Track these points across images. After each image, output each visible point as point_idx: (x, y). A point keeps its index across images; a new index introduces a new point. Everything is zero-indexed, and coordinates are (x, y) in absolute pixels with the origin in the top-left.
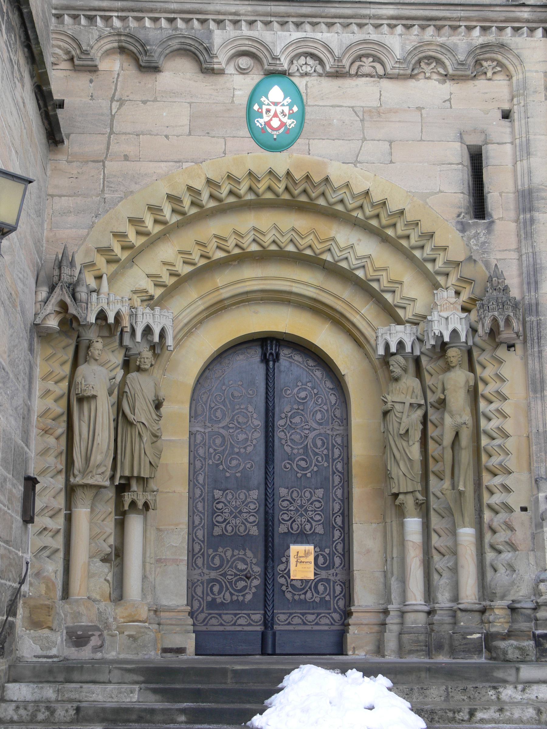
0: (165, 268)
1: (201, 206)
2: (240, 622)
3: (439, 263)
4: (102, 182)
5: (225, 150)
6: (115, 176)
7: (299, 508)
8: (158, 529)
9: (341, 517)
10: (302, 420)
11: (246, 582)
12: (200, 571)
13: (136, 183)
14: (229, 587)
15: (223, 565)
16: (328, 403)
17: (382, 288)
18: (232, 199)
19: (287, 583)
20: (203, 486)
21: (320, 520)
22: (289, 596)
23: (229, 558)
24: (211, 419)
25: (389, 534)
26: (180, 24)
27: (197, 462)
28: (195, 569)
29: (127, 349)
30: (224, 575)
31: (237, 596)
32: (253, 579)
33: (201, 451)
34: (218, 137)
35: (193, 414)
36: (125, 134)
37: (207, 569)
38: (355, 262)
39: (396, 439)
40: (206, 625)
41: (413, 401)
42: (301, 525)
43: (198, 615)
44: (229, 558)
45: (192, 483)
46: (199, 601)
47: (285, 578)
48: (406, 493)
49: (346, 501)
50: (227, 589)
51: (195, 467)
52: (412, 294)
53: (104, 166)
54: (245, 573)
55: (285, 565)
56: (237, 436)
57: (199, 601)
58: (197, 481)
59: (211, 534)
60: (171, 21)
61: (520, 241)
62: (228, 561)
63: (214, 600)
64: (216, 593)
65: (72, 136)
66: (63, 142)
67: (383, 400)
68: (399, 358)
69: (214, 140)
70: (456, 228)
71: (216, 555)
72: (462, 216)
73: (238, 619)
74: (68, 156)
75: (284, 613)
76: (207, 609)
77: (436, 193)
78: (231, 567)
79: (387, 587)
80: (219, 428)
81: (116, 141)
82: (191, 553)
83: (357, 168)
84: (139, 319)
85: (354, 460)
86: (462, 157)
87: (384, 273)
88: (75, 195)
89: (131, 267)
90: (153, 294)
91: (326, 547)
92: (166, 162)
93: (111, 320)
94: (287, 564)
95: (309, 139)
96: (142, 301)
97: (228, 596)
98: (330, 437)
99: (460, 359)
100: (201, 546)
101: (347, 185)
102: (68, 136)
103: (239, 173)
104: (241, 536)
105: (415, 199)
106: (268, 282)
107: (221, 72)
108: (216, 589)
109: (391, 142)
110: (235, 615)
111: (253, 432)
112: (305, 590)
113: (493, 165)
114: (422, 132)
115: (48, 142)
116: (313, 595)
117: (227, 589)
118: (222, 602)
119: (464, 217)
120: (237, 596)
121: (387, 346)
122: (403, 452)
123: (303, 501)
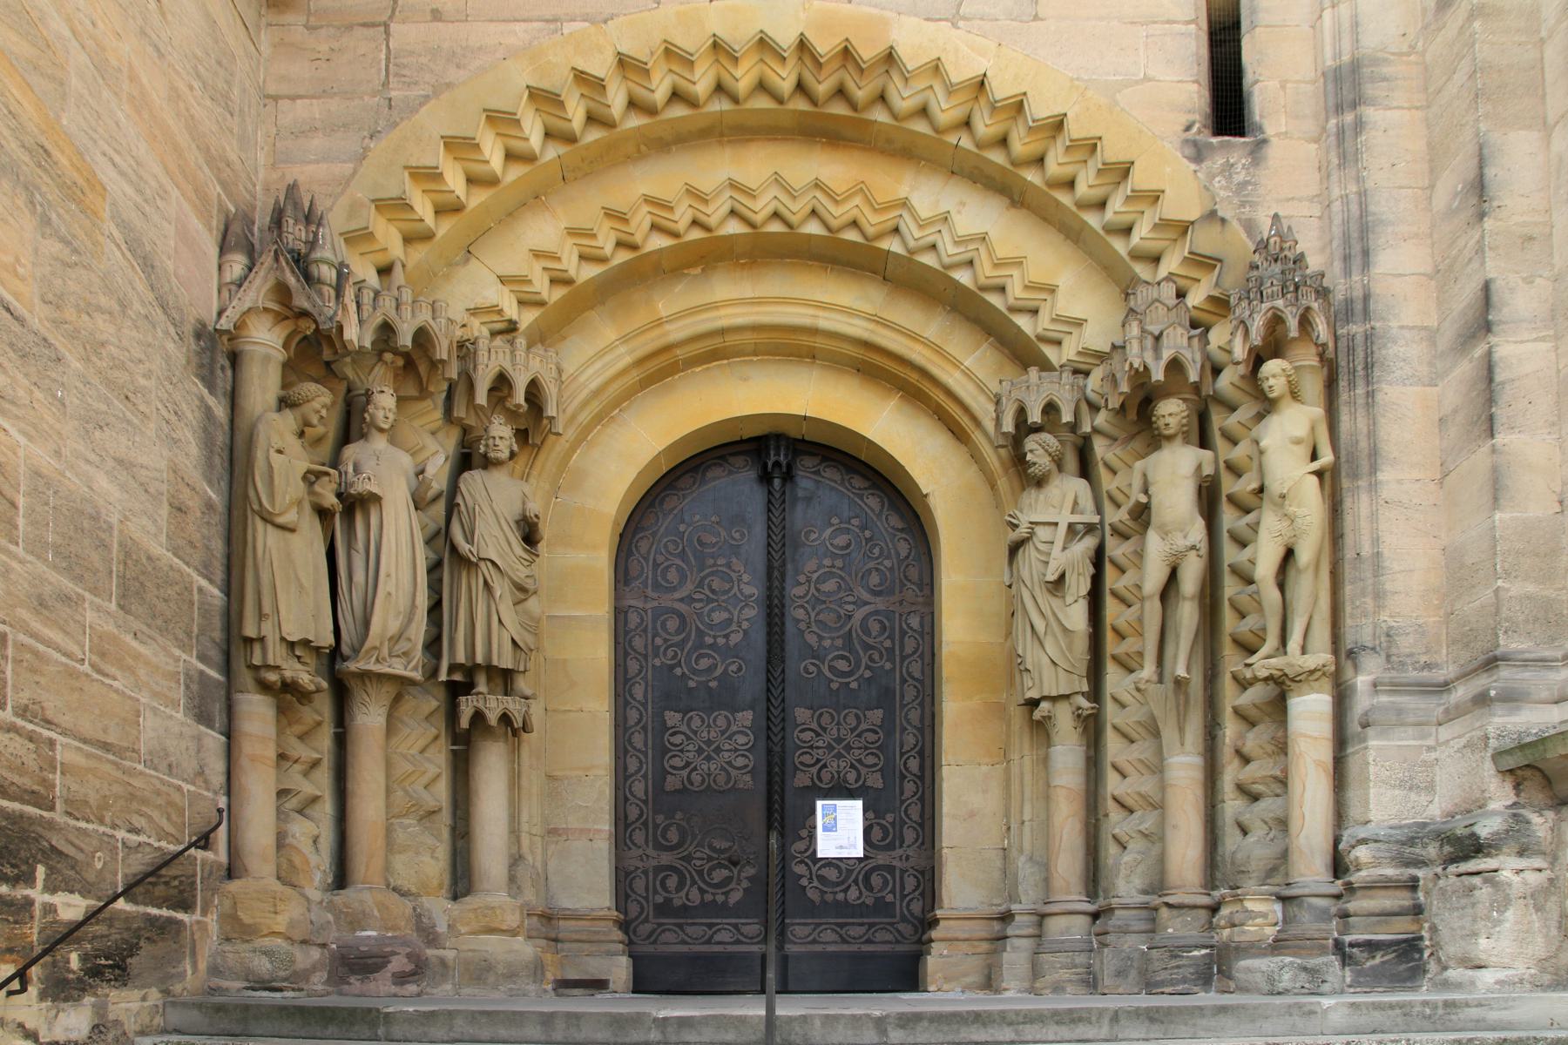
1: (608, 124)
3: (1142, 232)
4: (383, 67)
6: (412, 53)
8: (550, 777)
9: (918, 759)
11: (731, 870)
12: (640, 852)
14: (697, 878)
19: (811, 873)
25: (1015, 787)
30: (688, 859)
31: (713, 894)
32: (744, 866)
42: (839, 773)
46: (639, 902)
47: (807, 865)
49: (927, 731)
50: (694, 883)
53: (387, 33)
55: (806, 842)
57: (639, 902)
70: (1183, 153)
72: (1195, 129)
76: (656, 916)
77: (1137, 82)
83: (959, 31)
88: (324, 94)
92: (524, 21)
94: (810, 842)
97: (695, 895)
101: (936, 68)
103: (688, 42)
105: (1090, 94)
108: (672, 882)
113: (1267, 26)
117: (694, 883)
118: (684, 905)
119: (1199, 132)
120: (713, 894)
121: (1021, 412)
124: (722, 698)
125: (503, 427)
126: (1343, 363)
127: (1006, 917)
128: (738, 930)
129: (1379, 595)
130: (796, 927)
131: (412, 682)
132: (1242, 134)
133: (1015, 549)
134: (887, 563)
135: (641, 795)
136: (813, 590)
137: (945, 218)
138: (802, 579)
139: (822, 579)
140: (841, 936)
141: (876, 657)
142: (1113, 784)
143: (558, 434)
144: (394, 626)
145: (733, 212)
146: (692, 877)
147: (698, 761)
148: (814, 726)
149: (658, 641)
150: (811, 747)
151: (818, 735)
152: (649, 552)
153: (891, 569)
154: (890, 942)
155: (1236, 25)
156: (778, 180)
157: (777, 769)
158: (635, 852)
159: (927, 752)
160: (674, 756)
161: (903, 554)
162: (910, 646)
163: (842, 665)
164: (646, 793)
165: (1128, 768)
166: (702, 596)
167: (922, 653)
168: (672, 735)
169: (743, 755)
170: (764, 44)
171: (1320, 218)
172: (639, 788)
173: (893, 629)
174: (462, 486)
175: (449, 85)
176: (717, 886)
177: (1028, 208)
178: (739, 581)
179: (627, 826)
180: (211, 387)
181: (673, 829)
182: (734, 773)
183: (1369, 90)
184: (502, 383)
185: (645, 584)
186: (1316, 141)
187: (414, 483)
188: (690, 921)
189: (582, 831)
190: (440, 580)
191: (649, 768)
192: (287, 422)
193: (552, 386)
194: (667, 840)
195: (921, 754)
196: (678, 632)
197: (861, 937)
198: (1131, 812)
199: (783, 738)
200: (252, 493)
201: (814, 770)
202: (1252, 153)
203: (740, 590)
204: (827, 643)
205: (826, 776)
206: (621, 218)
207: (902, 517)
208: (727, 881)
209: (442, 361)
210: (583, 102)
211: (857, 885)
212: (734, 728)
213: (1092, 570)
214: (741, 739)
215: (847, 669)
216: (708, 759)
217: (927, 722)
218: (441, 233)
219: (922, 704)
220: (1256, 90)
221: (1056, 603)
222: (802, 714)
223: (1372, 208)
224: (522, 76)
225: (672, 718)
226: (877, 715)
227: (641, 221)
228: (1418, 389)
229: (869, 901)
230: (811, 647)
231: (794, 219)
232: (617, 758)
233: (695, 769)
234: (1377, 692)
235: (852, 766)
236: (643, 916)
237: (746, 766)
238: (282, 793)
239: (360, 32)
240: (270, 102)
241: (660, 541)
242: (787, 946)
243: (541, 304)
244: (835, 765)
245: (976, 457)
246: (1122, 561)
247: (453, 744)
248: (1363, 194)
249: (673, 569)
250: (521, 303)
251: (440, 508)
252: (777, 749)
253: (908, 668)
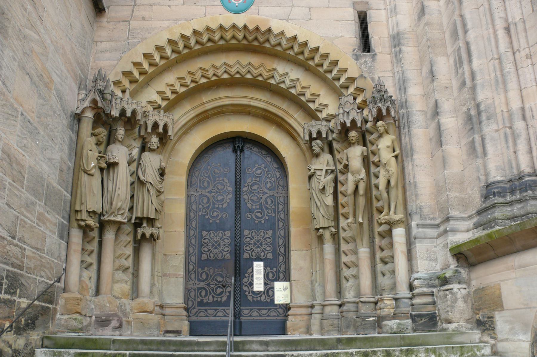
0: (168, 88)
2: (218, 314)
5: (205, 13)
7: (260, 246)
8: (164, 255)
10: (258, 187)
12: (193, 282)
13: (149, 33)
15: (207, 279)
16: (275, 177)
17: (307, 98)
18: (210, 44)
20: (196, 229)
21: (270, 250)
22: (250, 298)
23: (211, 274)
24: (200, 187)
27: (191, 214)
28: (190, 281)
29: (144, 139)
30: (209, 285)
32: (227, 287)
33: (194, 207)
34: (201, 6)
35: (189, 184)
36: (143, 5)
37: (198, 281)
38: (289, 83)
39: (317, 192)
40: (197, 316)
41: (328, 168)
43: (192, 310)
44: (211, 274)
45: (188, 227)
46: (192, 301)
47: (248, 287)
48: (324, 228)
50: (211, 293)
51: (190, 217)
52: (326, 103)
53: (129, 24)
54: (221, 283)
56: (217, 197)
58: (191, 225)
59: (200, 258)
61: (393, 65)
62: (211, 276)
63: (202, 300)
64: (203, 296)
65: (111, 8)
66: (104, 10)
67: (308, 169)
68: (318, 141)
69: (199, 7)
71: (203, 272)
73: (217, 312)
74: (108, 18)
75: (247, 309)
78: (213, 279)
79: (313, 290)
80: (206, 192)
81: (137, 9)
82: (187, 272)
84: (151, 117)
85: (291, 210)
86: (354, 17)
87: (308, 90)
89: (147, 87)
90: (160, 104)
91: (274, 267)
93: (129, 114)
95: (259, 6)
96: (154, 109)
98: (276, 197)
99: (357, 138)
100: (194, 266)
102: (108, 8)
104: (219, 260)
106: (235, 99)
108: (203, 294)
109: (310, 8)
110: (216, 310)
111: (227, 195)
112: (261, 294)
114: (329, 2)
115: (96, 11)
116: (266, 297)
117: (211, 293)
118: (207, 302)
119: (357, 51)
122: (322, 201)
123: (259, 238)
124: (220, 227)
125: (156, 139)
126: (401, 121)
128: (225, 312)
129: (416, 195)
130: (244, 310)
131: (124, 223)
132: (369, 52)
133: (310, 177)
134: (272, 179)
135: (194, 261)
136: (250, 189)
137: (287, 74)
138: (246, 185)
139: (252, 185)
140: (259, 314)
141: (270, 212)
142: (344, 259)
143: (172, 140)
144: (119, 204)
145: (225, 72)
146: (210, 291)
147: (213, 249)
148: (250, 236)
149: (201, 206)
150: (249, 244)
151: (251, 239)
152: (198, 176)
153: (274, 182)
154: (275, 316)
155: (366, 19)
156: (238, 62)
157: (238, 252)
158: (192, 282)
159: (287, 245)
160: (205, 247)
161: (278, 176)
162: (281, 207)
163: (259, 215)
164: (195, 261)
165: (347, 252)
166: (215, 191)
167: (284, 211)
168: (204, 239)
169: (227, 247)
170: (234, 26)
171: (392, 77)
172: (193, 259)
173: (275, 202)
174: (142, 157)
175: (146, 38)
176: (219, 295)
177: (311, 71)
178: (226, 185)
179: (189, 272)
180: (72, 130)
181: (204, 274)
182: (224, 253)
183: (402, 41)
184: (156, 125)
185: (197, 186)
186: (390, 54)
187: (128, 158)
188: (209, 308)
189: (175, 275)
190: (134, 188)
191: (197, 251)
192: (93, 140)
193: (170, 125)
194: (202, 278)
195: (285, 246)
196: (207, 203)
197: (266, 314)
198: (349, 268)
199: (240, 240)
200: (82, 164)
201: (250, 252)
202: (372, 58)
203: (227, 189)
204: (254, 207)
205: (254, 254)
206: (193, 74)
207: (277, 164)
208: (222, 293)
209: (139, 120)
210: (183, 42)
211: (264, 294)
212: (224, 237)
213: (334, 185)
214: (227, 241)
215: (261, 216)
216: (216, 248)
217: (287, 234)
218: (140, 80)
219: (285, 229)
220: (372, 39)
221: (323, 196)
222: (246, 232)
223: (405, 75)
225: (205, 233)
226: (270, 233)
227: (199, 74)
228: (423, 130)
229: (269, 301)
230: (249, 208)
231: (243, 74)
232: (186, 248)
233: (211, 252)
234: (418, 227)
235: (263, 251)
236: (194, 306)
237: (228, 251)
238: (82, 262)
239: (122, 23)
240: (95, 43)
241: (202, 172)
242: (241, 318)
243: (168, 99)
244: (257, 250)
245: (299, 145)
246: (343, 182)
247: (135, 244)
248: (403, 71)
249: (206, 182)
250: (162, 99)
251: (135, 164)
252: (238, 244)
253: (280, 216)
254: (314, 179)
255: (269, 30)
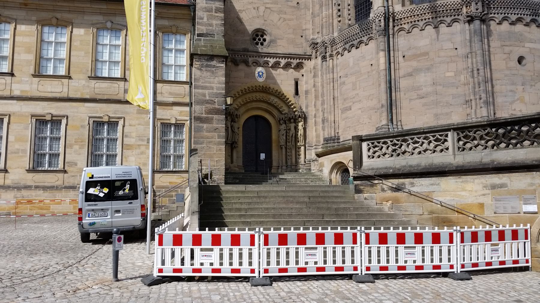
26: (243, 56)
60: (241, 56)
107: (250, 66)
127: (279, 166)
133: (279, 131)
142: (288, 154)
184: (237, 115)
224: (240, 89)
254: (281, 131)
255: (270, 87)
